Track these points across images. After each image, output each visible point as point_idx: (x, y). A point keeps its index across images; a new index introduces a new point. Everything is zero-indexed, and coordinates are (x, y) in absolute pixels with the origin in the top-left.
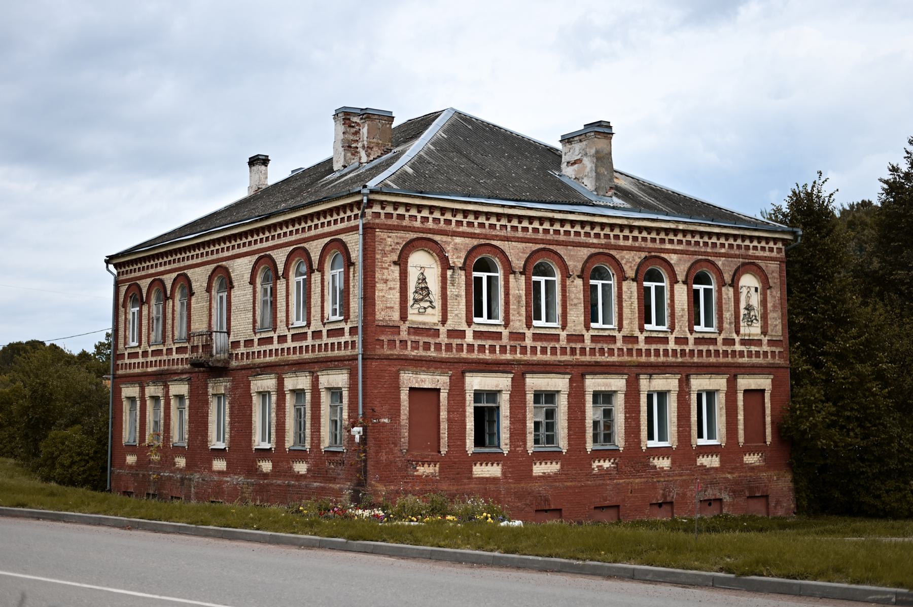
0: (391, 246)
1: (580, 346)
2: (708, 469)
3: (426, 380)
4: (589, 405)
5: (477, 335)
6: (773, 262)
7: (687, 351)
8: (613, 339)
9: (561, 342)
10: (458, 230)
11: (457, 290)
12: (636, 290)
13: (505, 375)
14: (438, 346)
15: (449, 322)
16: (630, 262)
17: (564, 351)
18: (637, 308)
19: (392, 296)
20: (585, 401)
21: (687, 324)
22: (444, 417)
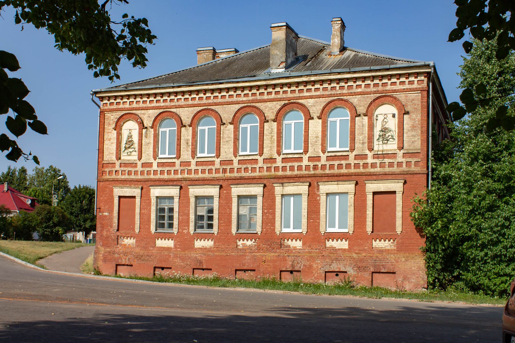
1: (230, 167)
2: (336, 250)
3: (127, 191)
4: (234, 205)
5: (159, 165)
6: (413, 92)
7: (320, 166)
8: (256, 161)
9: (216, 166)
10: (150, 106)
13: (175, 187)
14: (136, 173)
15: (143, 158)
18: (276, 139)
20: (232, 202)
21: (320, 147)
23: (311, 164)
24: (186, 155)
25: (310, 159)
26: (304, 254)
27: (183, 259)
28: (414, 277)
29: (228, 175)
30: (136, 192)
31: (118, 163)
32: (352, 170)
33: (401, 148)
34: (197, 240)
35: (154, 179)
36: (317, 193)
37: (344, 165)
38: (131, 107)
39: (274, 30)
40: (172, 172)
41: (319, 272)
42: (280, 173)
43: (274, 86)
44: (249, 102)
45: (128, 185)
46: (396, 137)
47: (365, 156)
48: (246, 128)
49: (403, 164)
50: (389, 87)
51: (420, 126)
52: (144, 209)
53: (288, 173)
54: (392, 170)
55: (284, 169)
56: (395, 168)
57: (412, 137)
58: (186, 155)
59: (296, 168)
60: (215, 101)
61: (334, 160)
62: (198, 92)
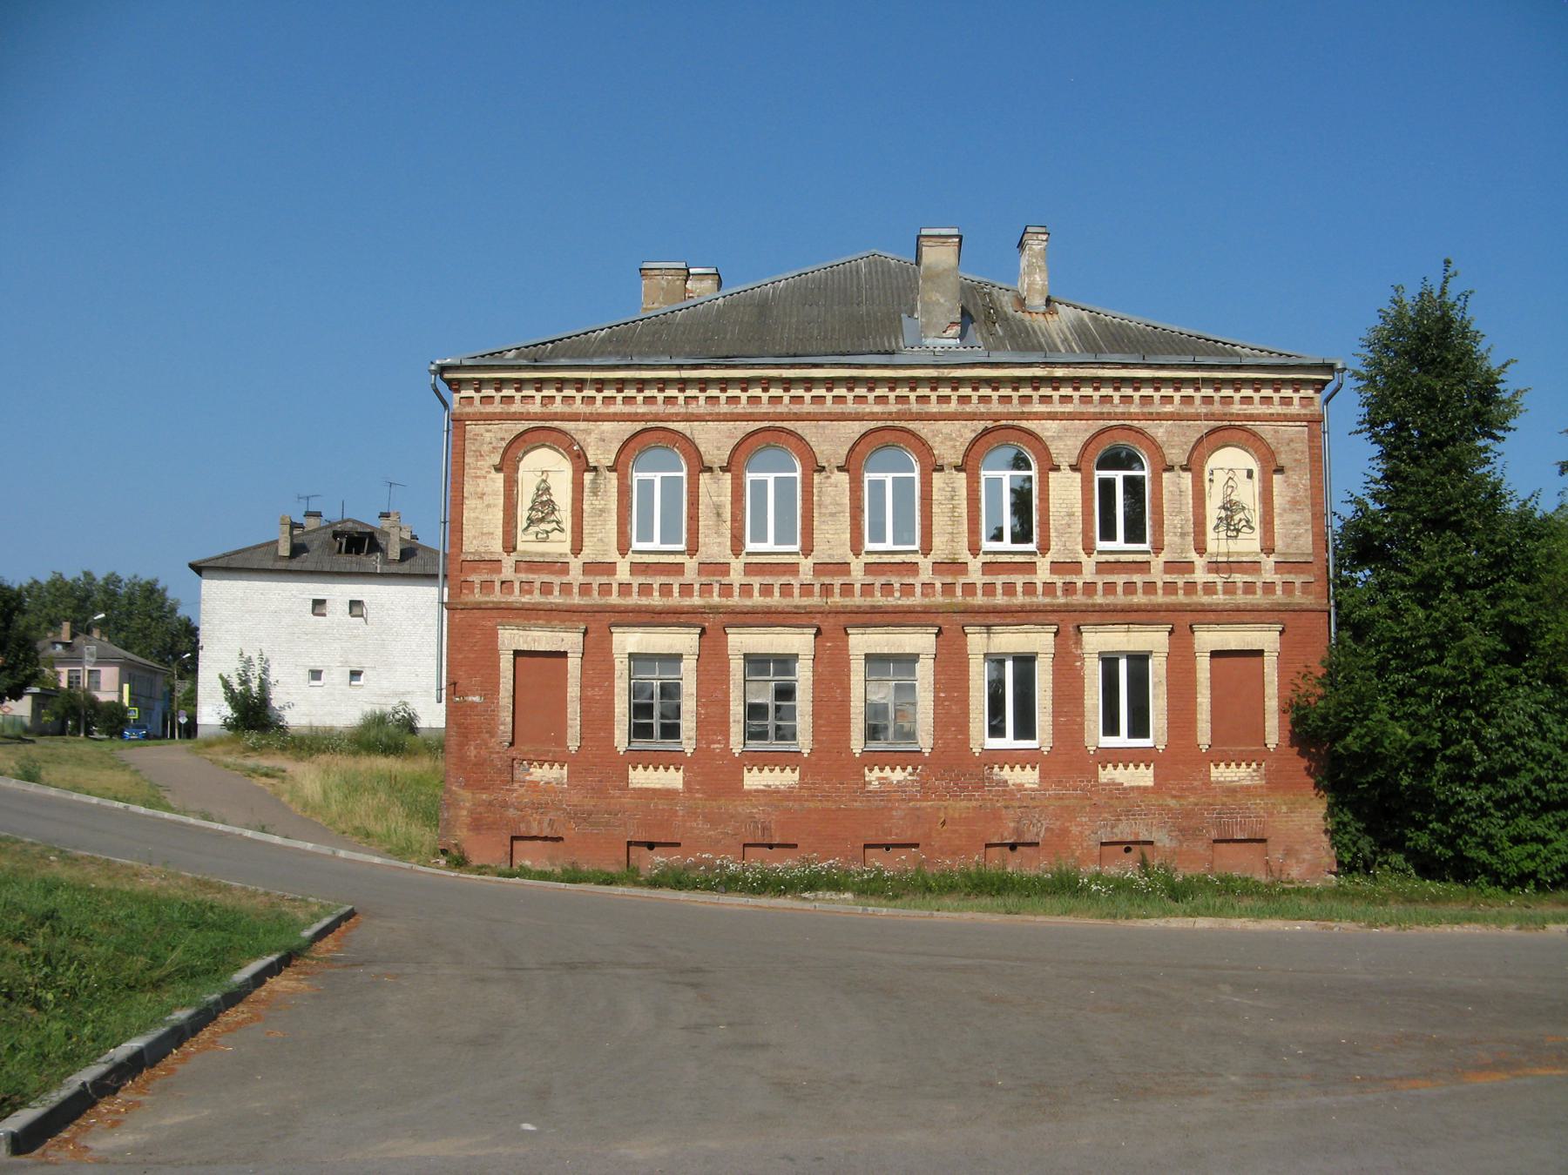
0: (491, 443)
1: (841, 582)
2: (1125, 789)
3: (541, 639)
4: (857, 678)
5: (636, 568)
6: (1290, 424)
7: (1080, 584)
8: (913, 568)
10: (606, 411)
11: (602, 502)
12: (965, 485)
13: (686, 630)
15: (586, 551)
16: (952, 439)
17: (806, 589)
18: (965, 515)
20: (849, 670)
21: (1080, 539)
22: (573, 695)
23: (1059, 580)
24: (715, 546)
25: (1056, 567)
26: (1046, 803)
27: (712, 819)
28: (1309, 849)
29: (837, 600)
30: (569, 640)
31: (508, 562)
32: (1160, 598)
33: (1268, 550)
34: (750, 770)
35: (620, 606)
36: (1074, 650)
37: (1139, 585)
38: (544, 410)
40: (676, 589)
41: (1085, 844)
42: (979, 600)
43: (956, 383)
44: (890, 416)
45: (540, 622)
46: (1256, 523)
47: (1188, 567)
48: (882, 484)
49: (1277, 588)
50: (1236, 408)
51: (1309, 502)
52: (593, 687)
53: (1000, 600)
54: (1255, 602)
55: (989, 589)
56: (1258, 596)
57: (1293, 527)
58: (715, 546)
59: (1019, 589)
60: (796, 408)
61: (1113, 573)
62: (745, 384)
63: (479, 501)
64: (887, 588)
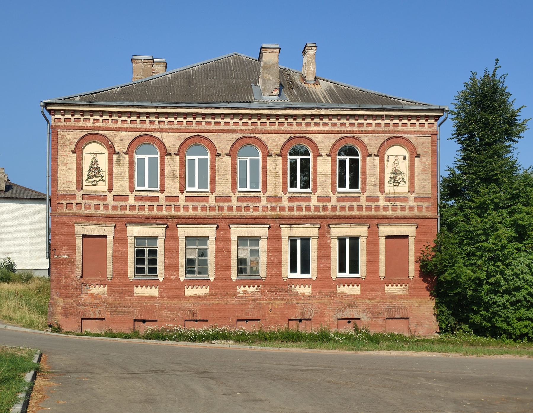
0: (70, 140)
1: (227, 205)
2: (348, 296)
3: (95, 230)
5: (137, 198)
6: (423, 135)
7: (330, 207)
9: (210, 202)
10: (123, 126)
11: (122, 168)
12: (281, 162)
15: (115, 190)
16: (276, 142)
17: (212, 208)
19: (71, 174)
22: (109, 254)
23: (321, 205)
24: (173, 189)
25: (320, 199)
26: (314, 301)
27: (171, 309)
28: (427, 322)
29: (225, 213)
30: (108, 230)
31: (79, 194)
32: (364, 213)
33: (412, 192)
34: (188, 287)
35: (130, 215)
36: (327, 235)
37: (355, 207)
38: (94, 125)
39: (266, 52)
40: (155, 208)
41: (331, 319)
42: (286, 213)
43: (278, 116)
44: (249, 131)
45: (94, 222)
46: (407, 180)
47: (377, 199)
49: (415, 208)
50: (400, 128)
51: (430, 170)
52: (118, 251)
53: (296, 213)
54: (404, 214)
55: (291, 208)
56: (406, 212)
57: (423, 181)
58: (173, 189)
59: (304, 208)
60: (208, 127)
61: (344, 202)
62: (186, 115)
63: (65, 167)
64: (247, 208)
